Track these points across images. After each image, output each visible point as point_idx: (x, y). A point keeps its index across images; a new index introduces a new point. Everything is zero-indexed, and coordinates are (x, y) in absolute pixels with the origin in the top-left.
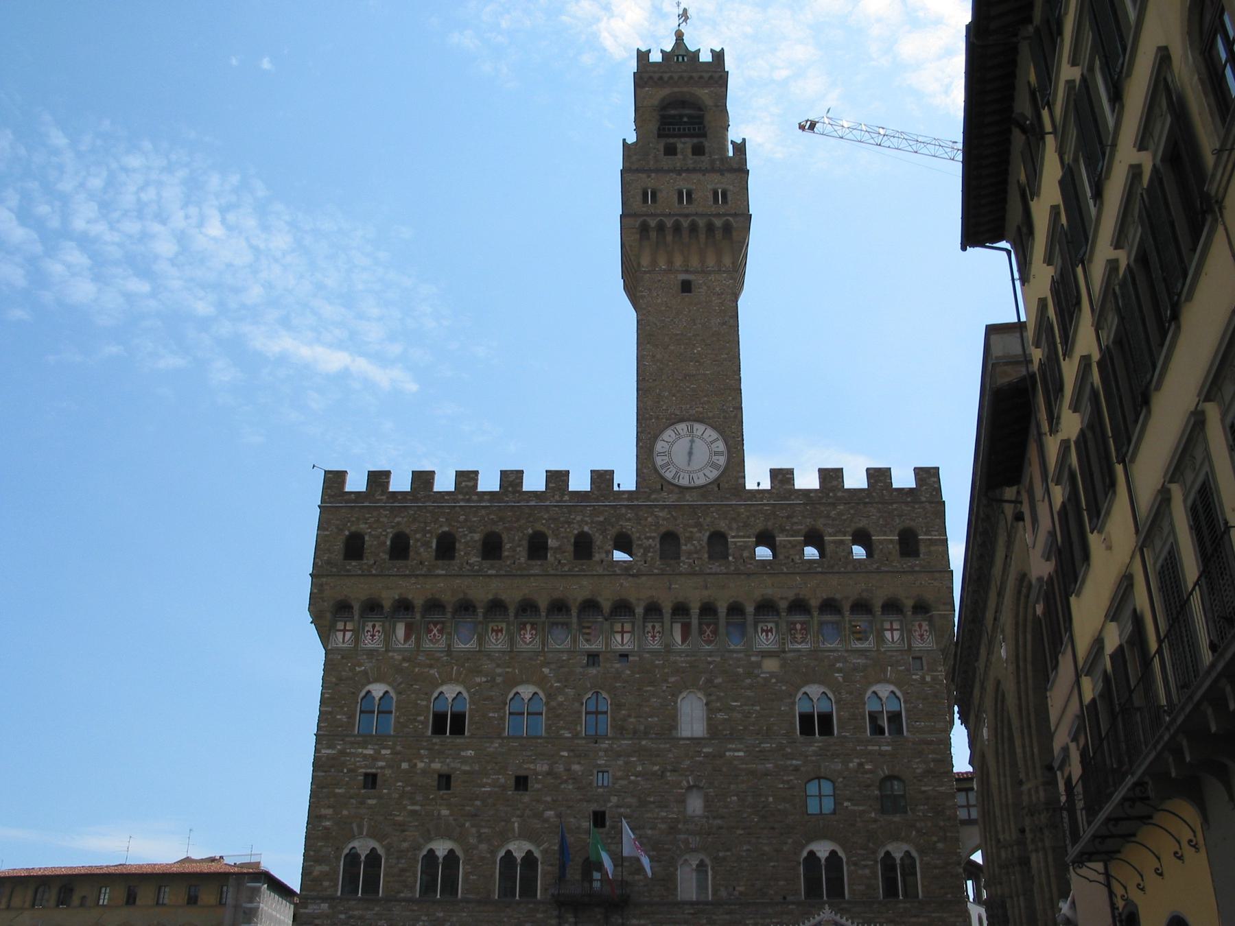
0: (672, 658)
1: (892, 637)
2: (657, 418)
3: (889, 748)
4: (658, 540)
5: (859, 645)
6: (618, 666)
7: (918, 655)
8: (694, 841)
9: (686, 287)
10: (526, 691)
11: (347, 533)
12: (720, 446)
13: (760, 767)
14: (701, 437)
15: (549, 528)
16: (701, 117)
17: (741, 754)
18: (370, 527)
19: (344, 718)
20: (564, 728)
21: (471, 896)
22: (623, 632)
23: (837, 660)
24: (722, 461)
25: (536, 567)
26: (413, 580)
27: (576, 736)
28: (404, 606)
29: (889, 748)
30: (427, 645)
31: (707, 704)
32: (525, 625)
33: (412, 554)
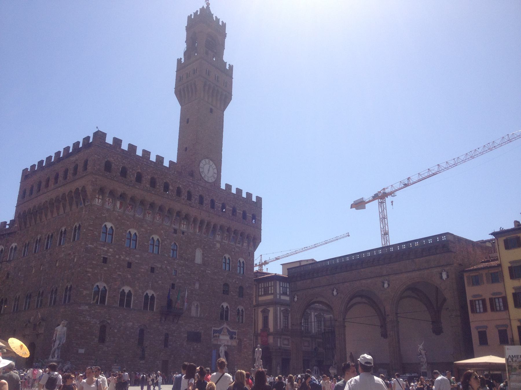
1: (245, 244)
5: (238, 245)
6: (182, 235)
9: (211, 111)
12: (216, 171)
18: (115, 160)
22: (184, 224)
24: (216, 176)
26: (128, 187)
28: (123, 197)
30: (127, 212)
31: (203, 254)
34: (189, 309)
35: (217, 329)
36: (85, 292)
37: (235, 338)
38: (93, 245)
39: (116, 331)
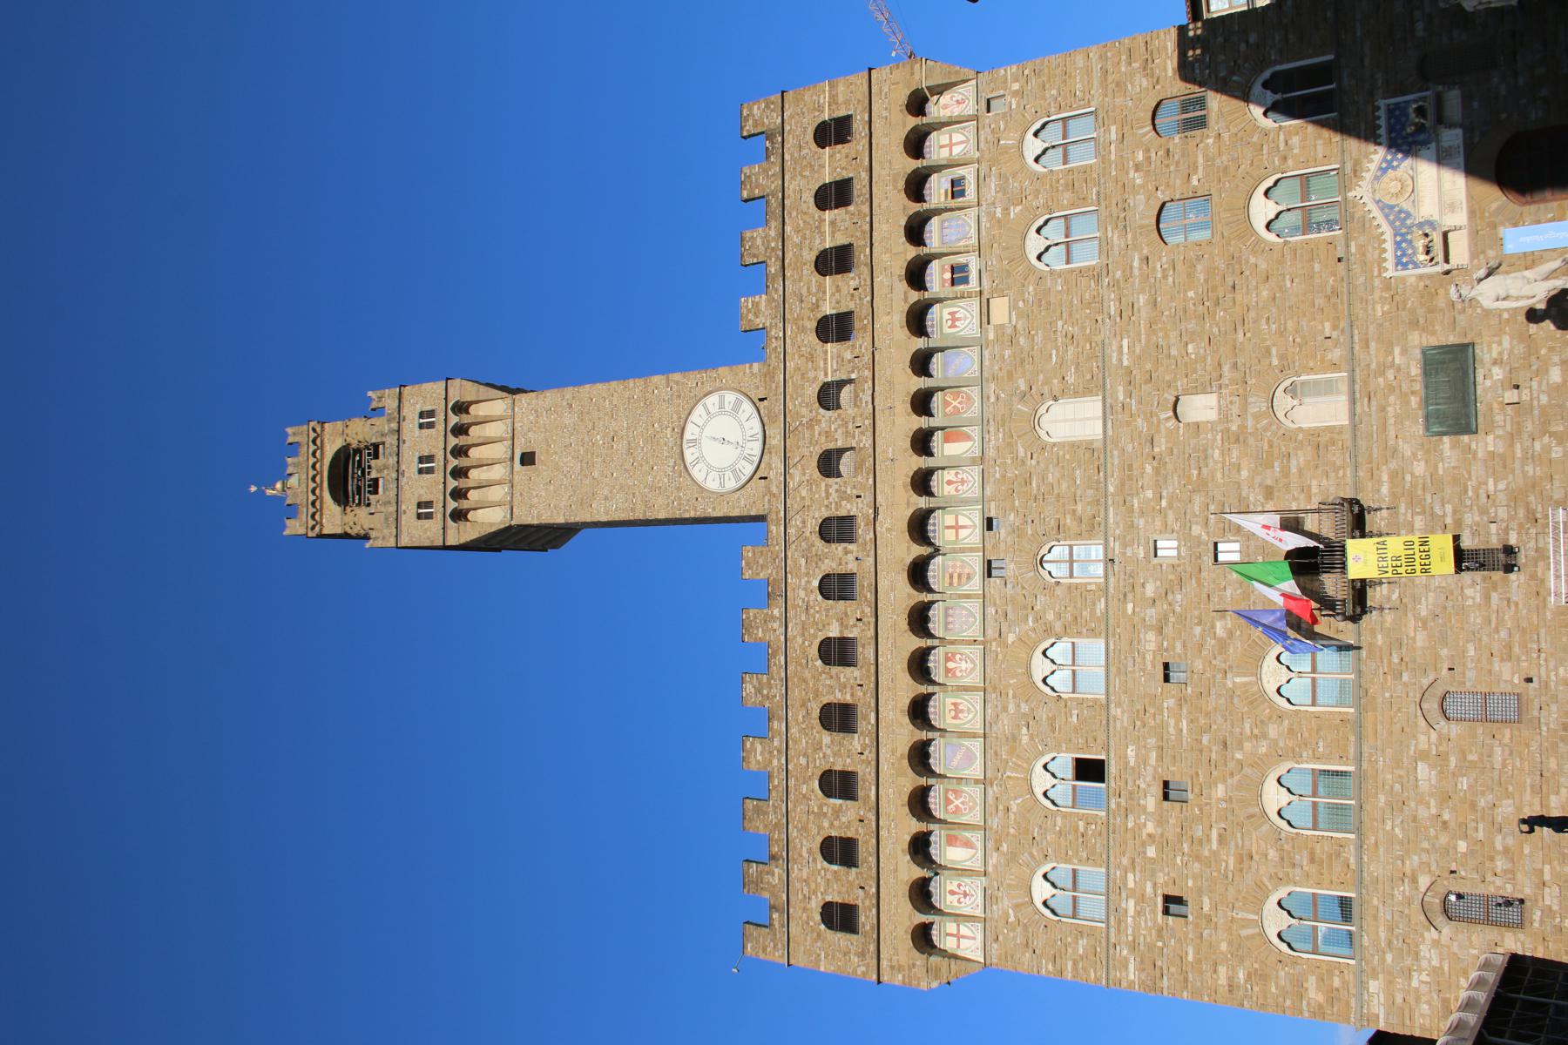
0: (991, 453)
2: (678, 489)
3: (1113, 129)
4: (831, 481)
6: (1001, 530)
7: (983, 104)
8: (1257, 404)
9: (528, 459)
10: (1040, 667)
11: (823, 927)
12: (712, 401)
13: (1143, 314)
14: (702, 428)
15: (815, 637)
16: (358, 451)
17: (1125, 343)
18: (815, 892)
19: (1083, 942)
20: (1093, 612)
21: (1352, 751)
22: (957, 527)
23: (992, 216)
24: (730, 397)
25: (865, 653)
27: (1104, 590)
28: (920, 847)
29: (1113, 129)
31: (1055, 399)
32: (948, 670)
33: (849, 835)
34: (1319, 441)
35: (1389, 246)
36: (1314, 994)
37: (1421, 112)
38: (1126, 960)
39: (1462, 846)
